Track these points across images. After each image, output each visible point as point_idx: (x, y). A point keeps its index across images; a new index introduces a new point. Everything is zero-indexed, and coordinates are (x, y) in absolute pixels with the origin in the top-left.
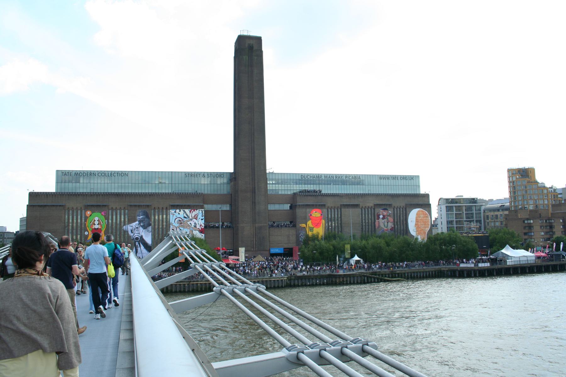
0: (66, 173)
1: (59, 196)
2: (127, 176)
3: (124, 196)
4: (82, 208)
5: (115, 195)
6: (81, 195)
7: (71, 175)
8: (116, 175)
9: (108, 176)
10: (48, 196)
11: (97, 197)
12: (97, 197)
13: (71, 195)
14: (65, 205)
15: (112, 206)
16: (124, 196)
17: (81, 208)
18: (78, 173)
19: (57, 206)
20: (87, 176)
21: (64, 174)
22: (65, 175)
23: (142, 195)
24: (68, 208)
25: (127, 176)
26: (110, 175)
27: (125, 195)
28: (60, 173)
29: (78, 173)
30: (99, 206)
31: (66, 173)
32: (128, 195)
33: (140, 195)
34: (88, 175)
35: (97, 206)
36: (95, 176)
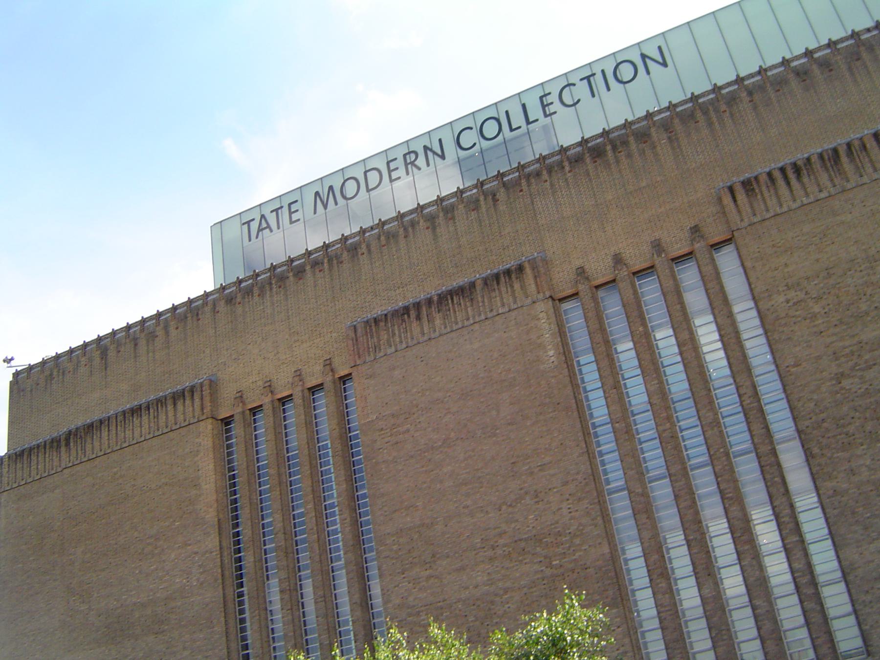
0: (263, 216)
1: (173, 332)
2: (665, 64)
3: (659, 137)
4: (336, 362)
5: (577, 160)
6: (316, 264)
7: (295, 217)
8: (583, 89)
9: (528, 122)
10: (112, 354)
11: (435, 237)
12: (435, 237)
13: (249, 292)
14: (213, 384)
15: (578, 263)
16: (659, 137)
17: (329, 364)
18: (331, 188)
19: (160, 402)
20: (391, 181)
21: (254, 226)
22: (260, 230)
23: (825, 65)
24: (240, 397)
25: (665, 64)
26: (535, 112)
27: (666, 126)
28: (235, 231)
29: (331, 188)
30: (465, 292)
31: (263, 216)
32: (688, 118)
33: (802, 74)
34: (394, 175)
35: (445, 299)
36: (443, 157)
